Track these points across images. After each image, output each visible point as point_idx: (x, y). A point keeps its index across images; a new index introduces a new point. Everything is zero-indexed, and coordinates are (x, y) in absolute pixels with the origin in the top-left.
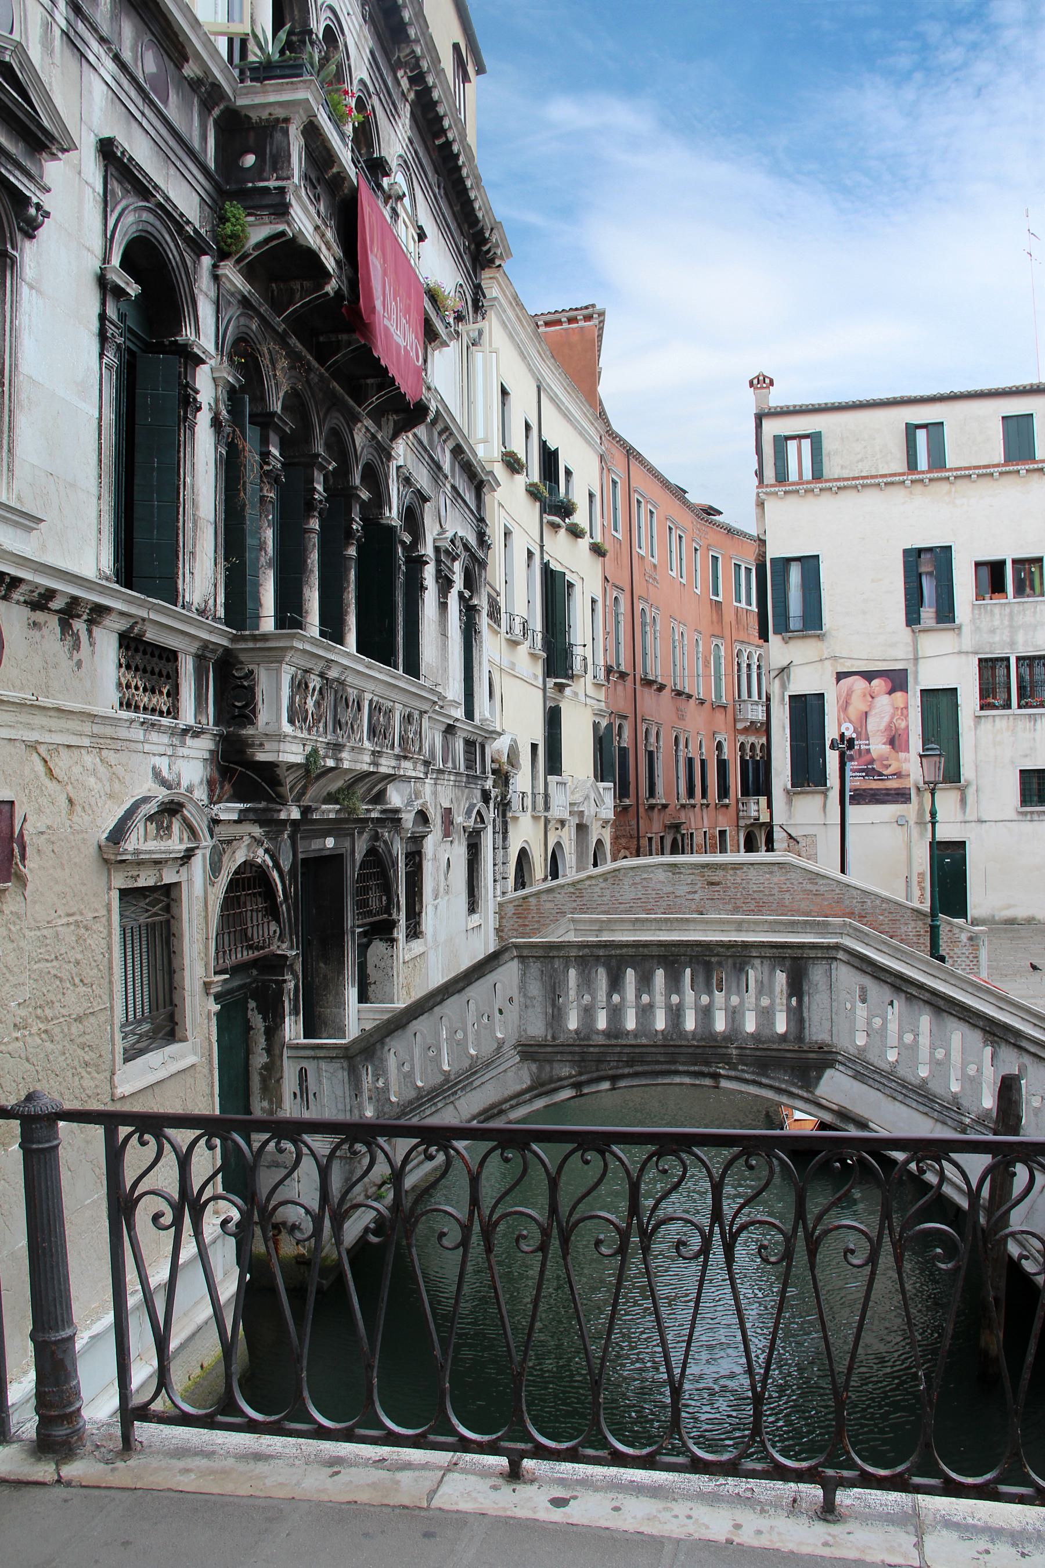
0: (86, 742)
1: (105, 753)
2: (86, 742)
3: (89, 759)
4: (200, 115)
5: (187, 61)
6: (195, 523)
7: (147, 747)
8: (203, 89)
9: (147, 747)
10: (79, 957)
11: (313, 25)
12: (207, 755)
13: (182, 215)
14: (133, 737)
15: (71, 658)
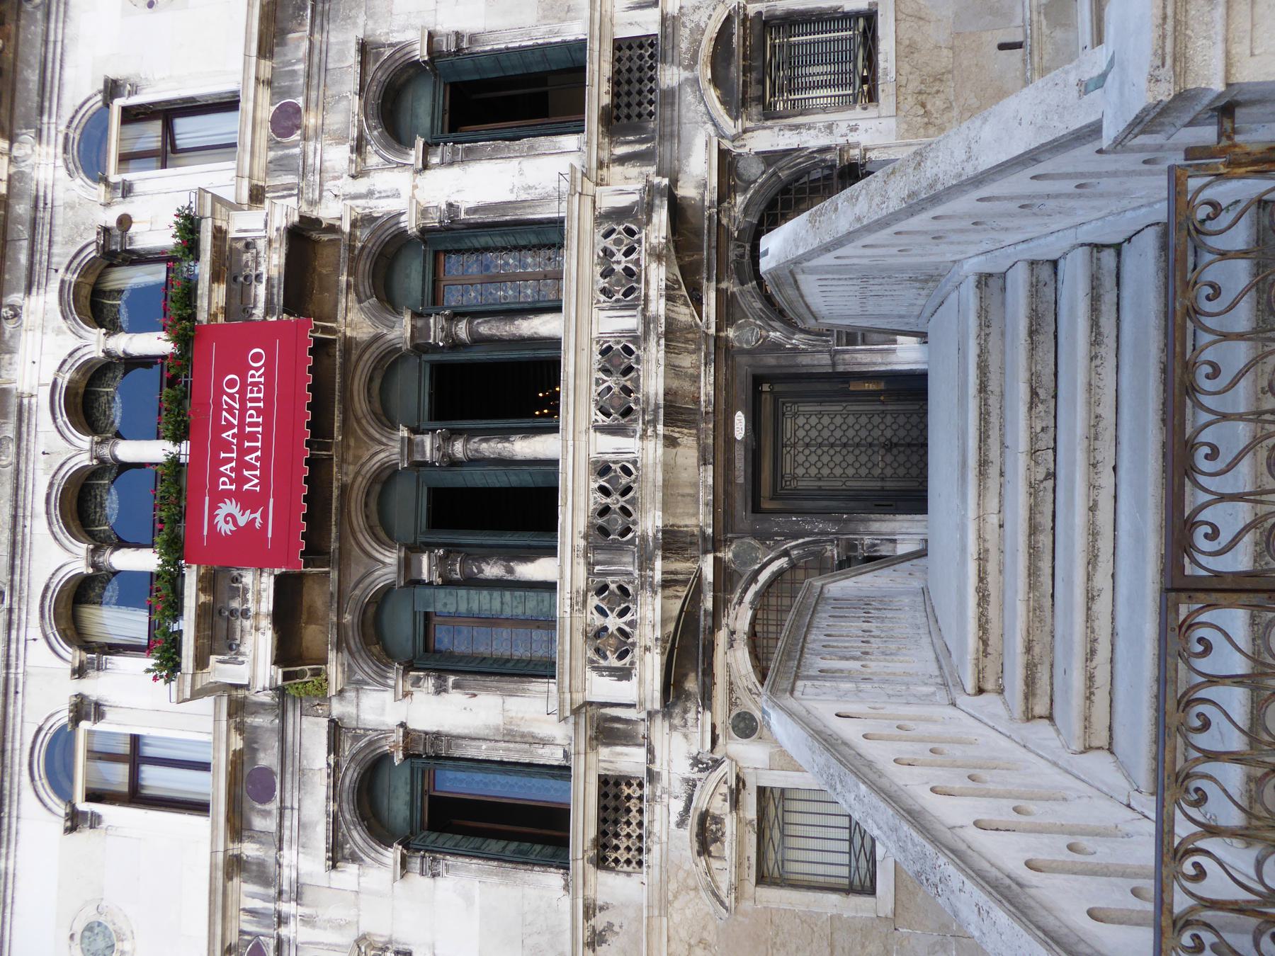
0: (665, 920)
1: (671, 897)
2: (665, 920)
3: (676, 918)
4: (254, 713)
5: (235, 751)
6: (510, 736)
7: (664, 838)
8: (238, 720)
9: (664, 838)
10: (794, 947)
11: (84, 460)
12: (667, 724)
13: (329, 776)
14: (659, 857)
15: (617, 933)
